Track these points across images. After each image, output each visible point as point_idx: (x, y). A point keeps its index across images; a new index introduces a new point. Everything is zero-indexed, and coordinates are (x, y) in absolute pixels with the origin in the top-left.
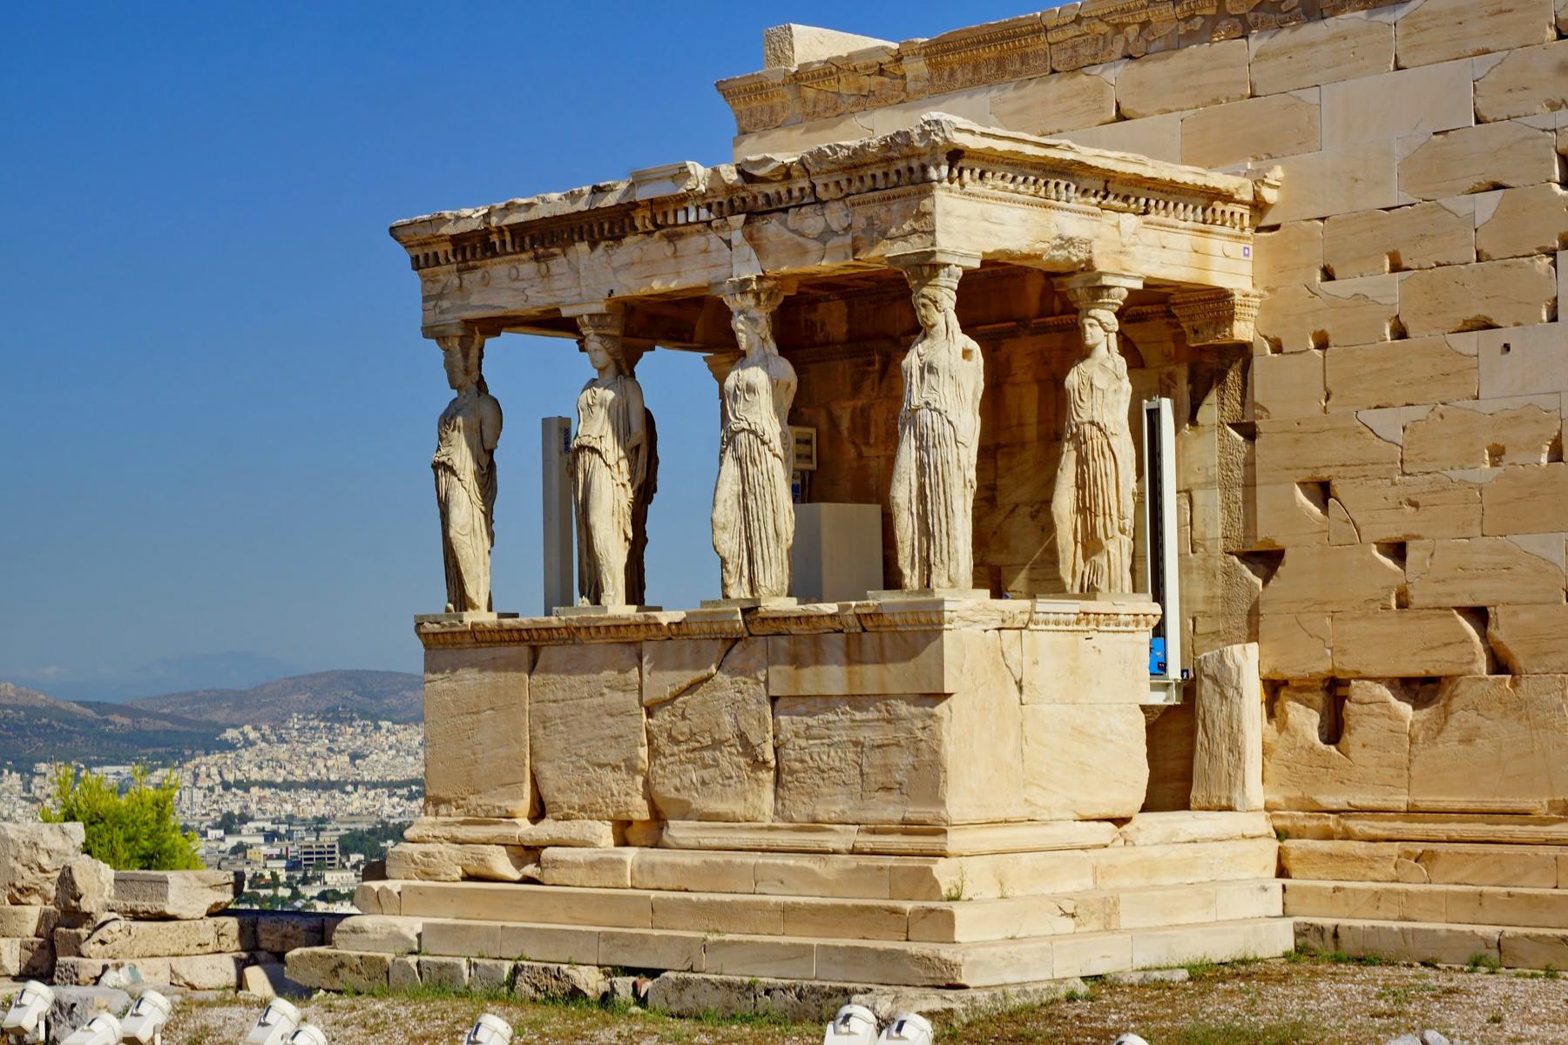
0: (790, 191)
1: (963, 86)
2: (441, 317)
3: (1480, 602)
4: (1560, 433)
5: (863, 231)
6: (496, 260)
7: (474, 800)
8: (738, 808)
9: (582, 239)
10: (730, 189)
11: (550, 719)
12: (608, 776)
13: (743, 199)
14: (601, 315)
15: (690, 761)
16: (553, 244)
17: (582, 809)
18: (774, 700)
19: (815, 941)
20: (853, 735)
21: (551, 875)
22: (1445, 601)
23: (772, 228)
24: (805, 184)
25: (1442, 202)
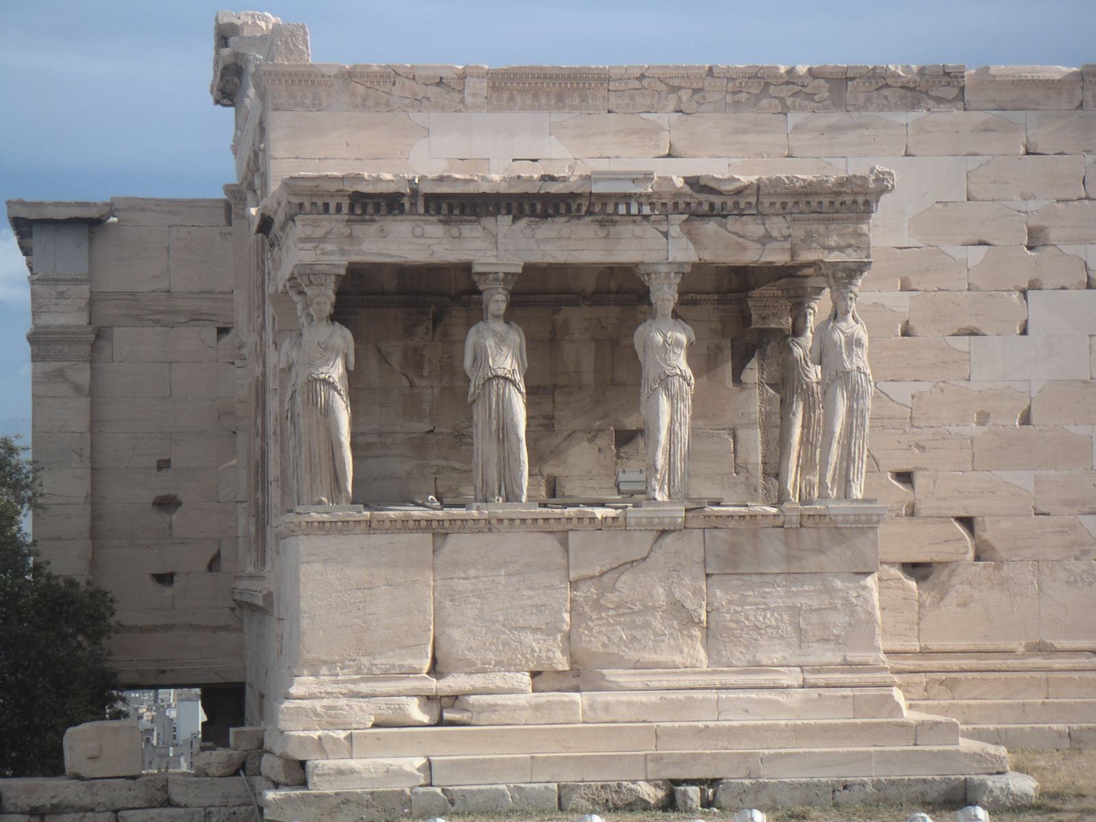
0: (736, 204)
1: (521, 109)
2: (321, 258)
3: (971, 513)
4: (1030, 407)
5: (803, 241)
6: (399, 218)
7: (365, 661)
8: (678, 659)
9: (509, 213)
10: (678, 194)
11: (460, 593)
12: (528, 638)
13: (688, 204)
14: (513, 274)
15: (619, 623)
16: (474, 213)
17: (498, 664)
18: (707, 575)
19: (872, 749)
20: (790, 602)
21: (483, 718)
22: (945, 512)
23: (711, 226)
24: (753, 200)
25: (943, 248)
